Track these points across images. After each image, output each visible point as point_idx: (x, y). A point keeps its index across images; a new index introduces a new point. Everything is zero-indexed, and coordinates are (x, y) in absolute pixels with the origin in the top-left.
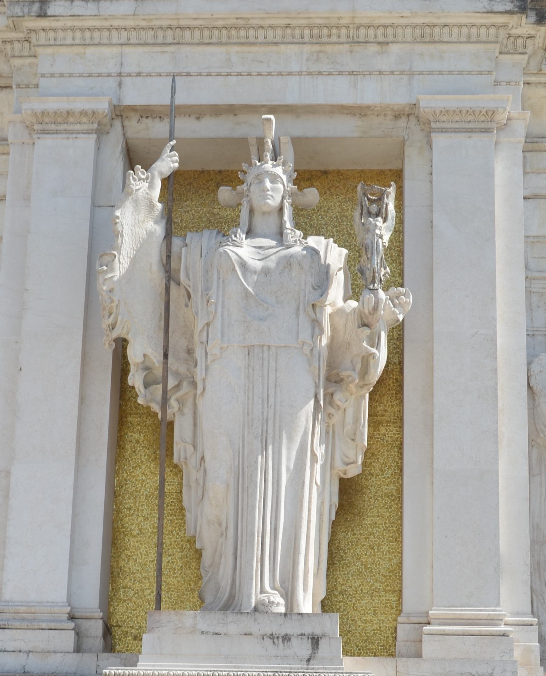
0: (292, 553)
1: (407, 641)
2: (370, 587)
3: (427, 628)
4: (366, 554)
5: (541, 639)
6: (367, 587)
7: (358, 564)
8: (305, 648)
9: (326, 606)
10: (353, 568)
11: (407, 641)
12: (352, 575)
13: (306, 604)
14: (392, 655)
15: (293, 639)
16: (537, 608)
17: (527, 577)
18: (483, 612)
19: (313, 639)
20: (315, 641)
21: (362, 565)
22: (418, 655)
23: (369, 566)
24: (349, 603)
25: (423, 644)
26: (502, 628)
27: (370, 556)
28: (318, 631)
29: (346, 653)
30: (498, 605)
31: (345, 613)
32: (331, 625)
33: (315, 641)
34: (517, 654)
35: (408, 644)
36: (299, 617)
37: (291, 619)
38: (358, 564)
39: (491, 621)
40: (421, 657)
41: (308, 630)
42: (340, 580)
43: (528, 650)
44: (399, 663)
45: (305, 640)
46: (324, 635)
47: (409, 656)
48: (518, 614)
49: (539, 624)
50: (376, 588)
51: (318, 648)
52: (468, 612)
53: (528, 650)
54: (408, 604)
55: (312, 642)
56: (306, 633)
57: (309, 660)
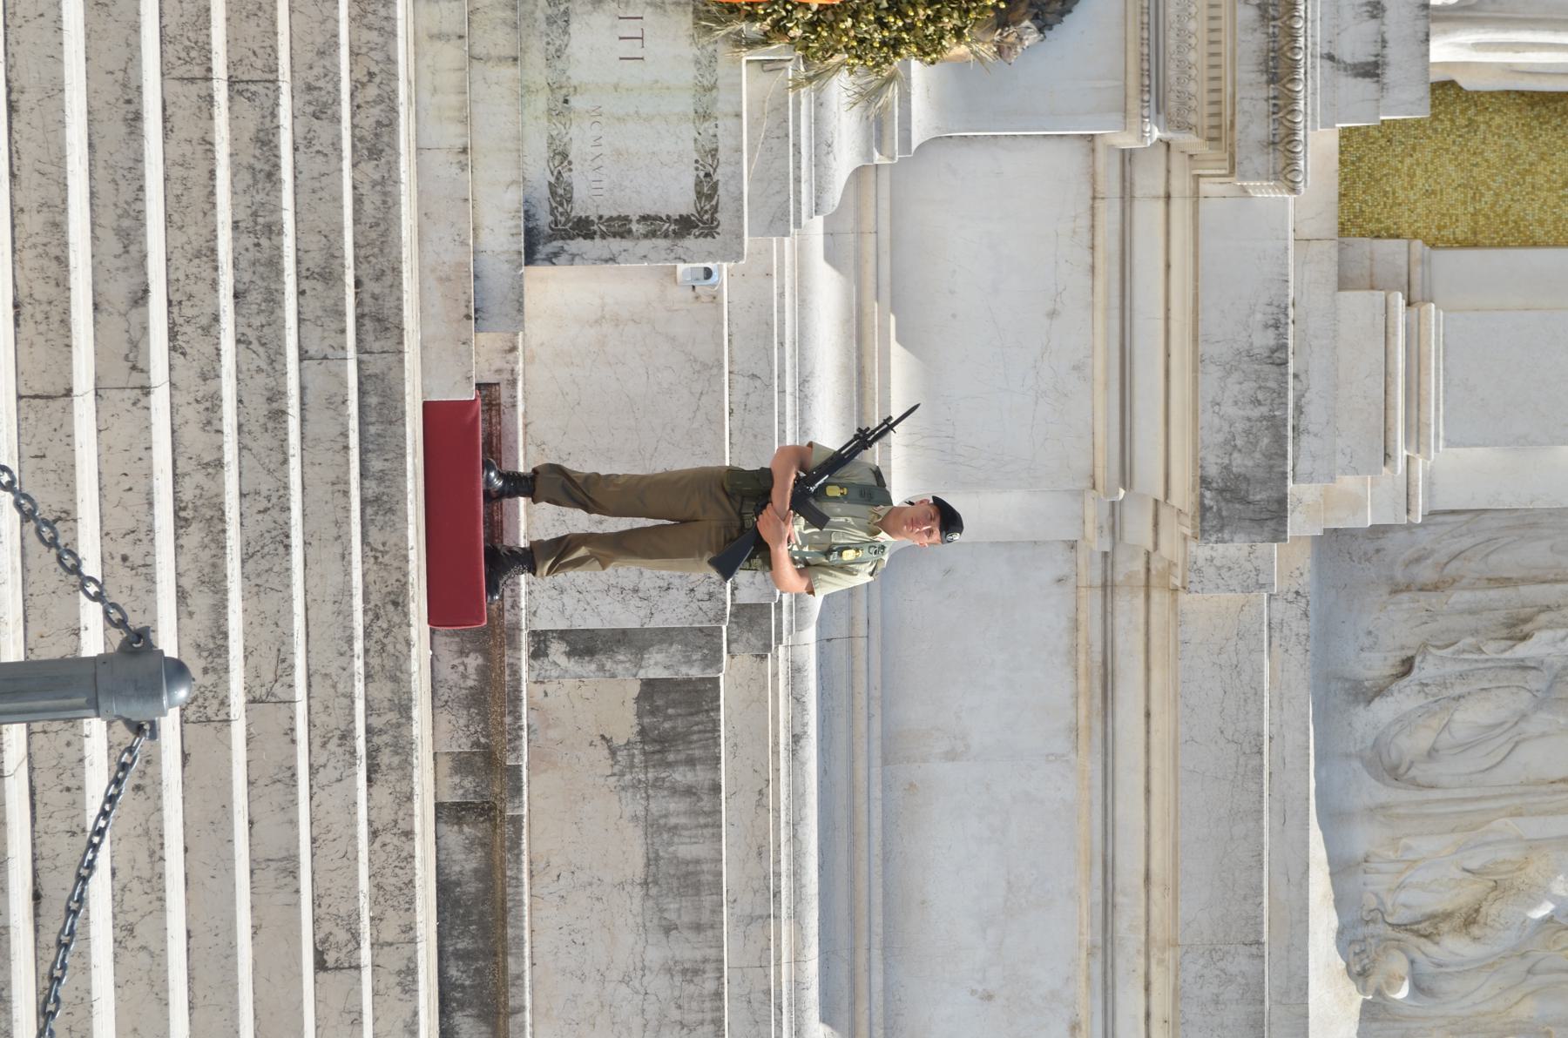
0: (1555, 16)
1: (1372, 260)
2: (1484, 183)
3: (1399, 300)
4: (1553, 172)
5: (1378, 531)
6: (1484, 176)
7: (1533, 157)
8: (1355, 48)
9: (1445, 91)
10: (1523, 147)
11: (1372, 260)
12: (1508, 145)
13: (1450, 50)
14: (1343, 230)
15: (1373, 24)
16: (1442, 523)
17: (1507, 501)
18: (1434, 413)
19: (1376, 65)
20: (1371, 70)
21: (1531, 164)
22: (1344, 283)
23: (1529, 179)
24: (1449, 140)
25: (1366, 293)
26: (1401, 452)
27: (1548, 181)
28: (1391, 75)
29: (1346, 135)
30: (1450, 443)
31: (1429, 132)
32: (1405, 103)
33: (1371, 70)
34: (1348, 482)
35: (1367, 263)
36: (1421, 36)
37: (1417, 18)
38: (1533, 157)
39: (1415, 431)
40: (1340, 289)
41: (1394, 54)
42: (1498, 120)
43: (1357, 505)
44: (1327, 245)
45: (1373, 49)
46: (1383, 87)
47: (1340, 264)
48: (1430, 483)
49: (1410, 527)
50: (1482, 195)
51: (1357, 75)
52: (1433, 384)
53: (1357, 505)
54: (1451, 262)
55: (1368, 64)
56: (1387, 51)
57: (1331, 58)
